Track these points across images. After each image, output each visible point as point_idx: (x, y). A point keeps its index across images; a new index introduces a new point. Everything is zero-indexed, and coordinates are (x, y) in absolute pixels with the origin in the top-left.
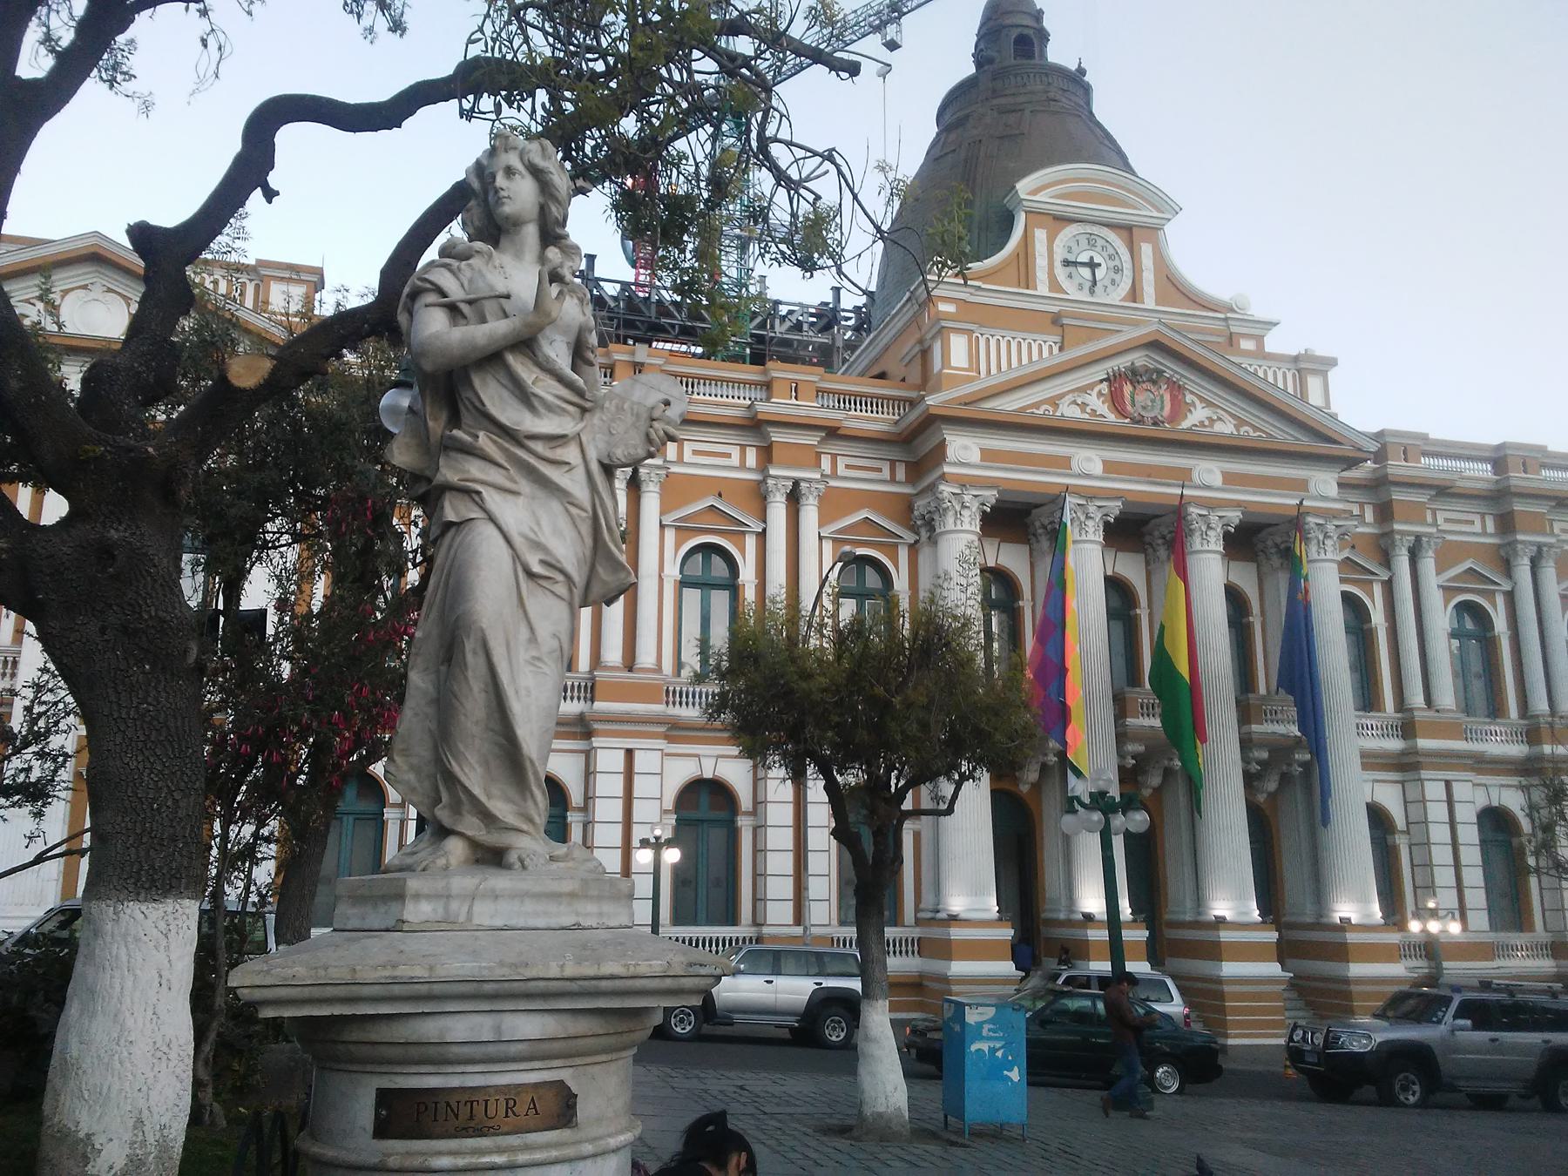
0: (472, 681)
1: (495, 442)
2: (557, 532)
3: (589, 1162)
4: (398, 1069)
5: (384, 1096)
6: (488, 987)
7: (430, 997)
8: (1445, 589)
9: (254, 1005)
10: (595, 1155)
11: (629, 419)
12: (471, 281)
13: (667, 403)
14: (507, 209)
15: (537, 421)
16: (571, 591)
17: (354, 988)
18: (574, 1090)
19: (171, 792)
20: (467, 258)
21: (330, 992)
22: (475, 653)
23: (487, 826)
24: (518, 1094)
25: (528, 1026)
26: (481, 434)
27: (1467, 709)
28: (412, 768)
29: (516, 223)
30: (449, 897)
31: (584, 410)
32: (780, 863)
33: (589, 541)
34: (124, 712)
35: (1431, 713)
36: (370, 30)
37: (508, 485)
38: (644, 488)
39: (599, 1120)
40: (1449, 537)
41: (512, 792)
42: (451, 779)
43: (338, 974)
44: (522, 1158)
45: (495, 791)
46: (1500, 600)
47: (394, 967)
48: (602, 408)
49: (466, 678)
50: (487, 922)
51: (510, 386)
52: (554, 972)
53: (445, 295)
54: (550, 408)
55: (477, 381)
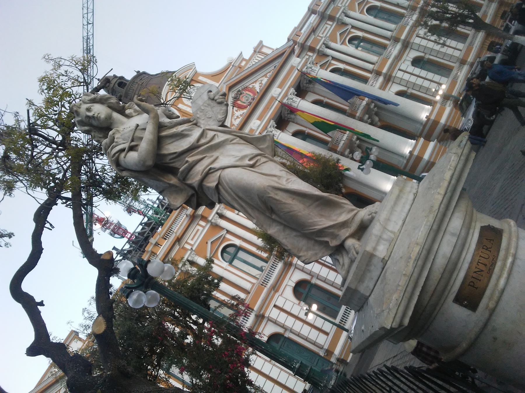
0: (287, 202)
4: (449, 288)
5: (459, 300)
6: (435, 227)
7: (429, 252)
8: (342, 44)
9: (401, 324)
11: (209, 109)
12: (124, 140)
14: (103, 116)
16: (265, 157)
17: (412, 279)
20: (114, 139)
21: (409, 289)
22: (276, 194)
23: (348, 227)
26: (187, 159)
27: (380, 54)
28: (307, 250)
29: (109, 118)
30: (380, 237)
31: (196, 124)
35: (377, 64)
36: (6, 244)
37: (212, 159)
38: (195, 260)
40: (328, 35)
41: (338, 211)
42: (322, 232)
43: (403, 281)
45: (335, 218)
46: (353, 30)
47: (410, 258)
49: (285, 203)
50: (398, 227)
51: (173, 140)
52: (440, 198)
53: (123, 150)
55: (165, 152)
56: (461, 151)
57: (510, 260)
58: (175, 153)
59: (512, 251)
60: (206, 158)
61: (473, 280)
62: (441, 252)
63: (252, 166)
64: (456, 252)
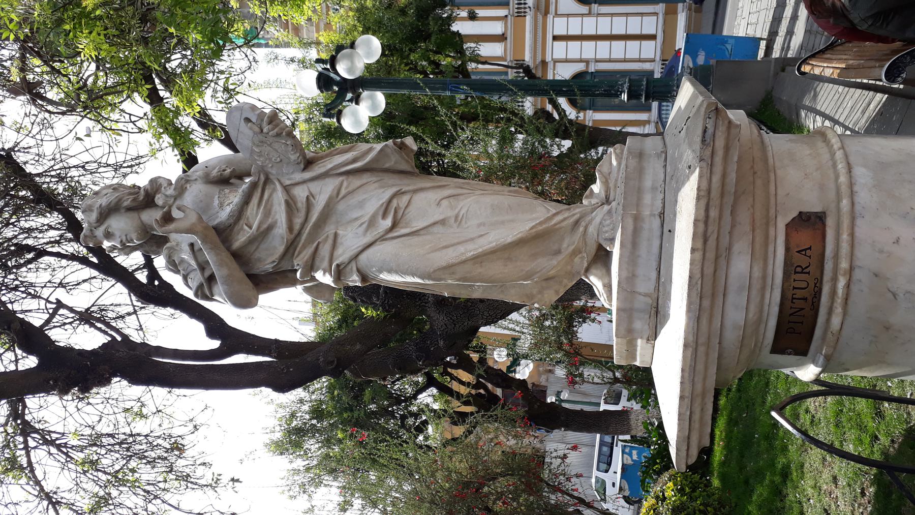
1: (300, 253)
2: (361, 205)
3: (857, 199)
10: (852, 194)
15: (279, 224)
16: (403, 193)
18: (795, 214)
24: (792, 265)
25: (740, 265)
32: (618, 49)
33: (366, 178)
37: (330, 241)
39: (822, 187)
44: (844, 265)
48: (262, 167)
51: (256, 244)
54: (268, 213)
56: (710, 149)
57: (842, 283)
58: (274, 262)
59: (844, 265)
60: (321, 245)
61: (791, 325)
62: (728, 323)
64: (753, 308)
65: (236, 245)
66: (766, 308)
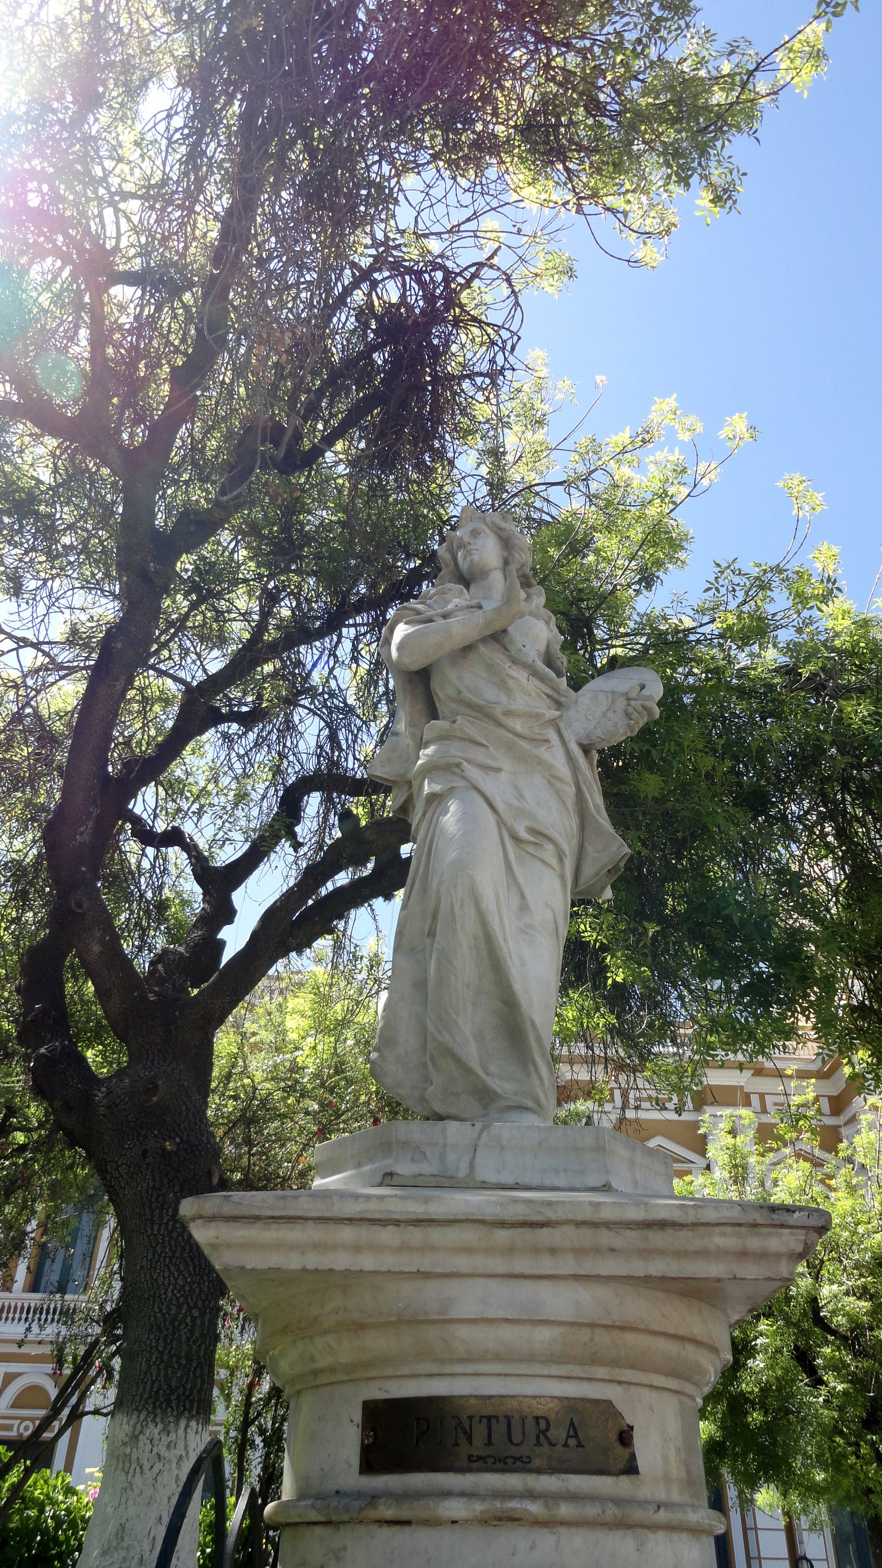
13: (643, 687)
16: (561, 860)
19: (190, 1310)
34: (156, 1227)
37: (489, 762)
50: (492, 1178)
60: (483, 749)
63: (516, 839)
65: (482, 649)
66: (470, 1368)
